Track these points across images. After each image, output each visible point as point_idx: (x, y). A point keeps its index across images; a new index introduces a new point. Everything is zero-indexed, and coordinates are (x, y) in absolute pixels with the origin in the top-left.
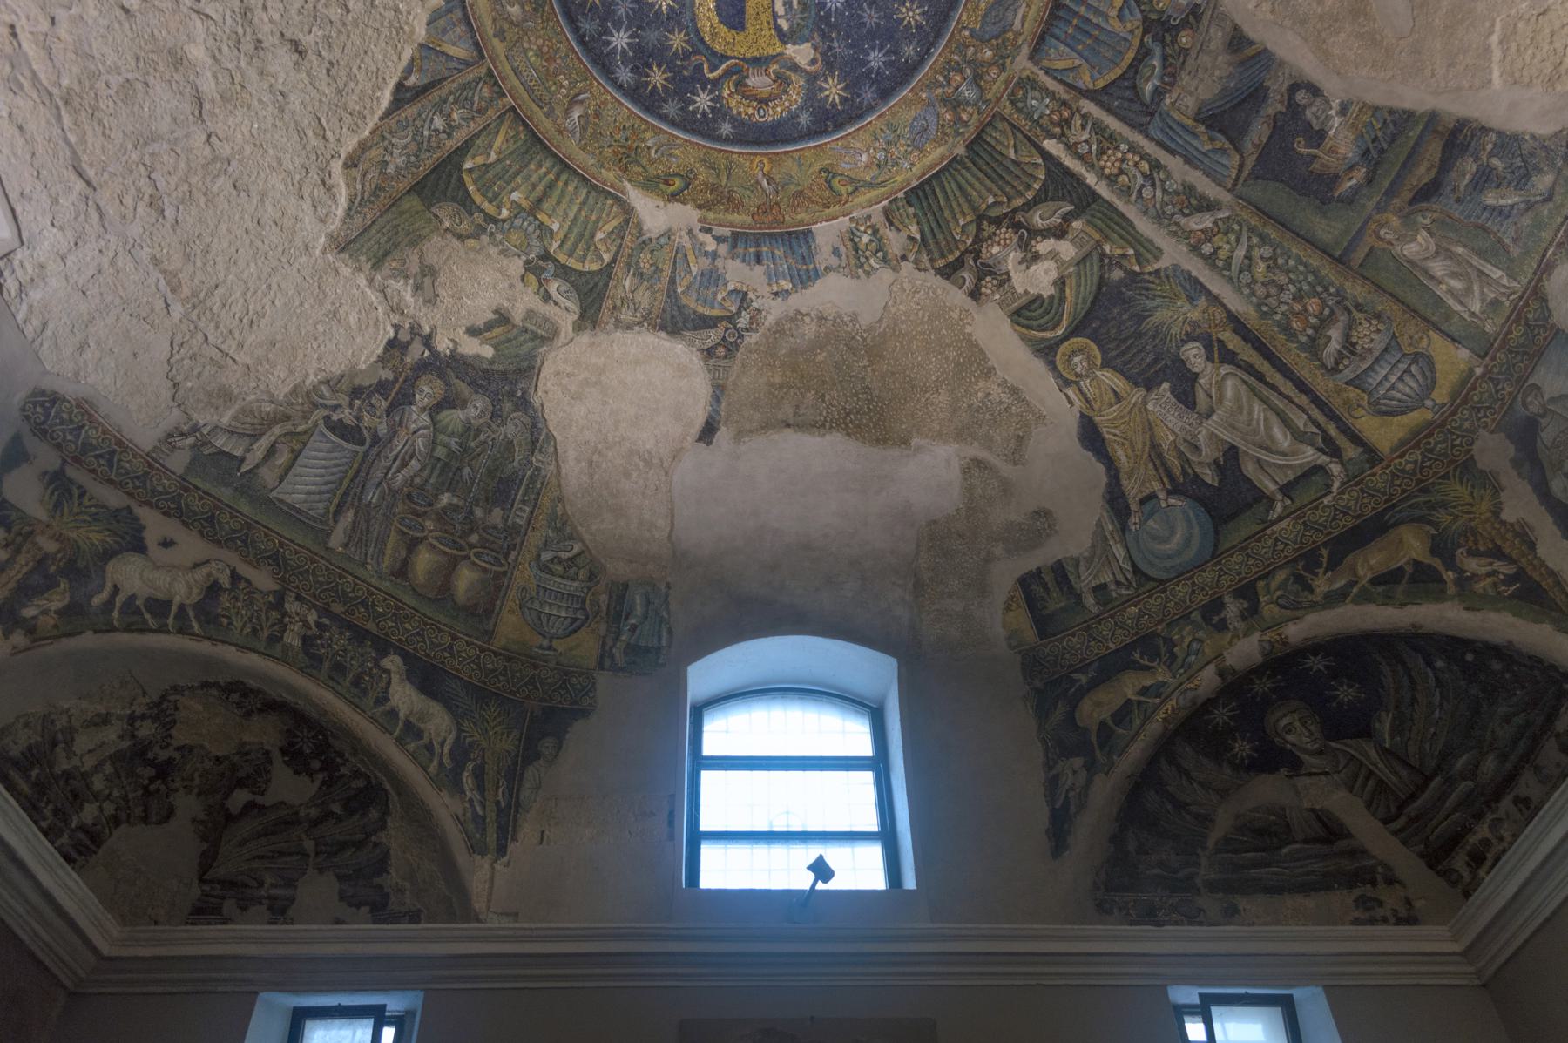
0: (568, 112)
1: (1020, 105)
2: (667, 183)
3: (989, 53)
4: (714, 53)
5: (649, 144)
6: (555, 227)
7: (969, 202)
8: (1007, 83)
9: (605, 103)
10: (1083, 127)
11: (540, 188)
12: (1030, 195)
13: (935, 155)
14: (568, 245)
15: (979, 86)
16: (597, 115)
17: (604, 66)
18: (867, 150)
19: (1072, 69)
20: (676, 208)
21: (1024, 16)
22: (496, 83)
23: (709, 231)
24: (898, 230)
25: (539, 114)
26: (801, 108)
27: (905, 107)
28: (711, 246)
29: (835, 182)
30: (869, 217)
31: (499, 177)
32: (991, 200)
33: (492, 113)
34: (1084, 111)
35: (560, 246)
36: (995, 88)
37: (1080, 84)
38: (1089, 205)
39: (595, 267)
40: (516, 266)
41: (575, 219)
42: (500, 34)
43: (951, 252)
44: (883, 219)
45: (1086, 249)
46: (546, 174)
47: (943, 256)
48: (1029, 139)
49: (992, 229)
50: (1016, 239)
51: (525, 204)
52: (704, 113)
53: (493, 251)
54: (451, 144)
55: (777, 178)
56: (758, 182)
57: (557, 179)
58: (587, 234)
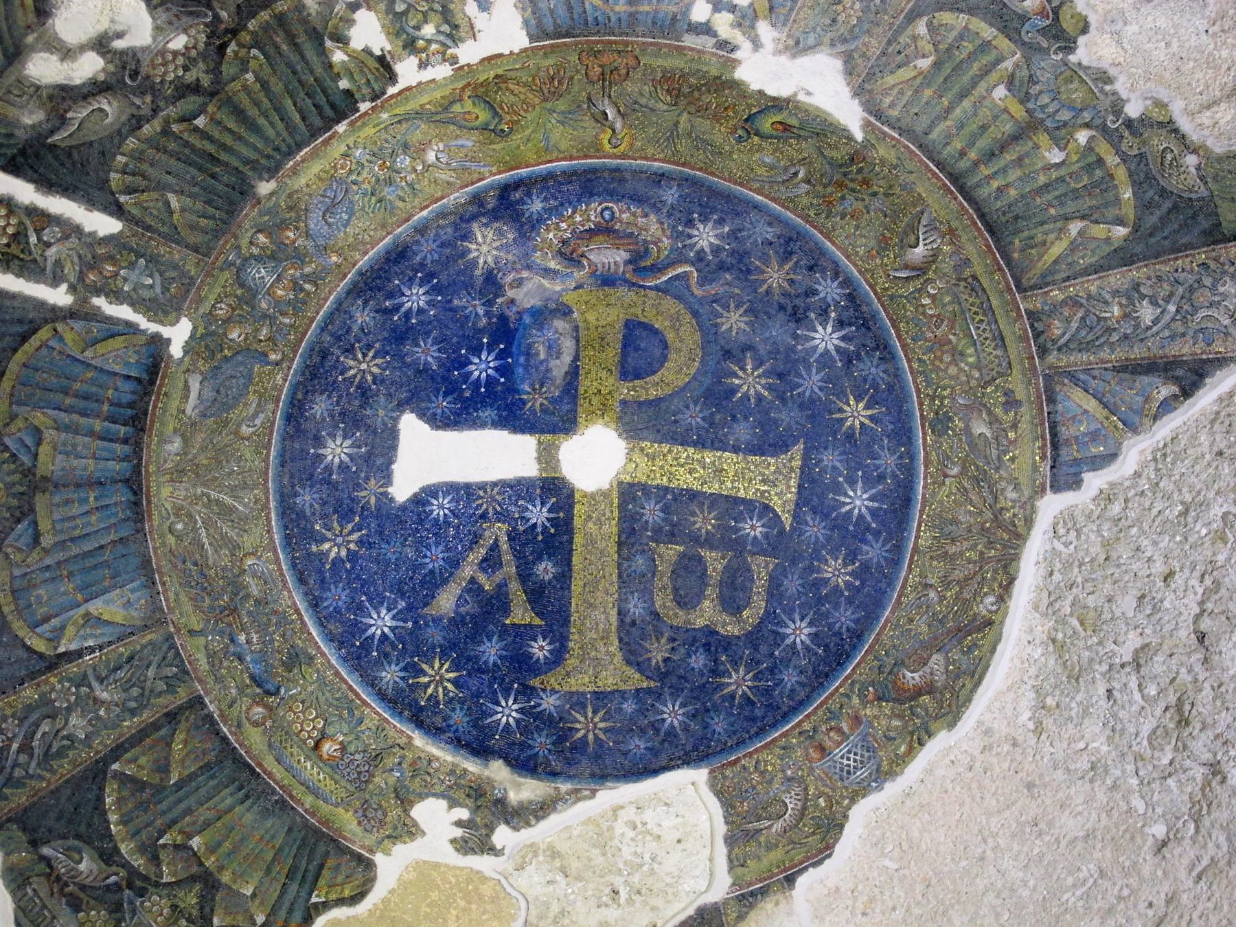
0: (935, 255)
1: (171, 274)
2: (787, 127)
3: (234, 335)
4: (678, 297)
5: (805, 187)
6: (1000, 92)
7: (239, 113)
8: (200, 300)
9: (869, 256)
10: (58, 263)
11: (1009, 157)
12: (131, 143)
13: (309, 171)
14: (986, 59)
15: (242, 285)
16: (883, 245)
17: (857, 308)
18: (427, 167)
19: (95, 342)
20: (777, 88)
21: (186, 397)
22: (1037, 335)
23: (724, 45)
24: (367, 51)
25: (978, 267)
26: (540, 220)
27: (364, 239)
28: (723, 24)
29: (483, 115)
30: (422, 65)
31: (1075, 194)
32: (200, 122)
33: (1056, 294)
34: (64, 287)
35: (999, 61)
36: (218, 290)
37: (78, 325)
38: (23, 152)
39: (947, 17)
40: (1086, 52)
41: (963, 95)
42: (1011, 403)
43: (266, 27)
44: (399, 68)
45: (9, 79)
46: (989, 178)
47: (280, 18)
48: (148, 228)
49: (190, 77)
50: (145, 69)
51: (1043, 139)
52: (705, 219)
53: (1121, 86)
54: (1138, 273)
55: (588, 121)
56: (623, 116)
57: (976, 164)
58: (947, 70)
